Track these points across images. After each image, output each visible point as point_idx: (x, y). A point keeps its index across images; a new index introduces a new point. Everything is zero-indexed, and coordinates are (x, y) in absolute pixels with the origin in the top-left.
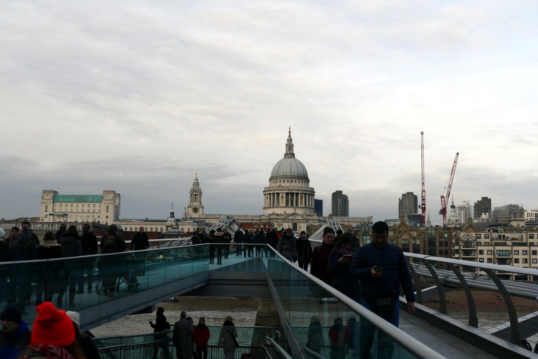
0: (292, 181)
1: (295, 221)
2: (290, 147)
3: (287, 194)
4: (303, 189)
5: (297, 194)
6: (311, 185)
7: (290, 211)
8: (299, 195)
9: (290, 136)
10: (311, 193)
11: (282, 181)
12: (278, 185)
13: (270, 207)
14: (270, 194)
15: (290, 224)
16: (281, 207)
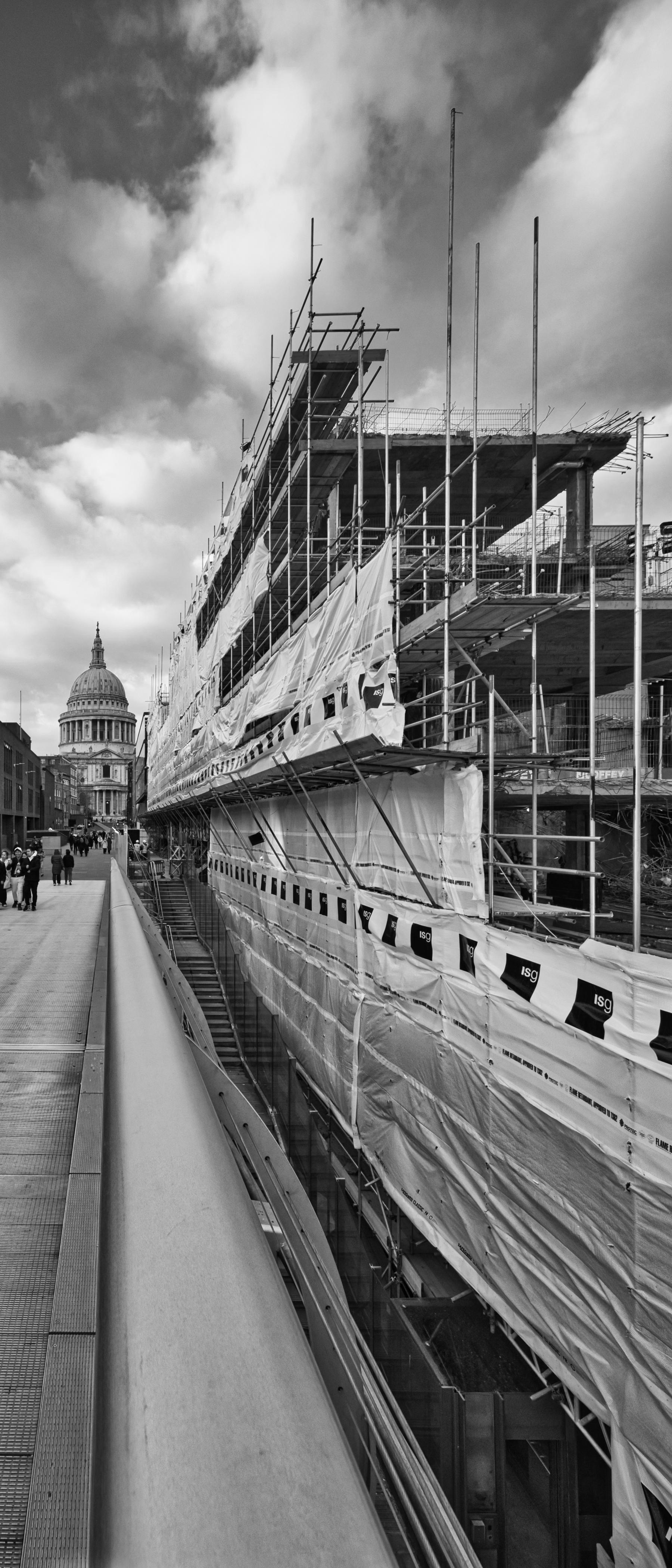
0: (101, 702)
1: (107, 762)
2: (98, 652)
3: (94, 722)
4: (118, 714)
5: (110, 722)
6: (130, 709)
7: (98, 747)
8: (113, 724)
9: (98, 636)
10: (132, 721)
11: (86, 703)
12: (79, 708)
13: (68, 743)
14: (68, 723)
15: (98, 767)
16: (85, 742)
